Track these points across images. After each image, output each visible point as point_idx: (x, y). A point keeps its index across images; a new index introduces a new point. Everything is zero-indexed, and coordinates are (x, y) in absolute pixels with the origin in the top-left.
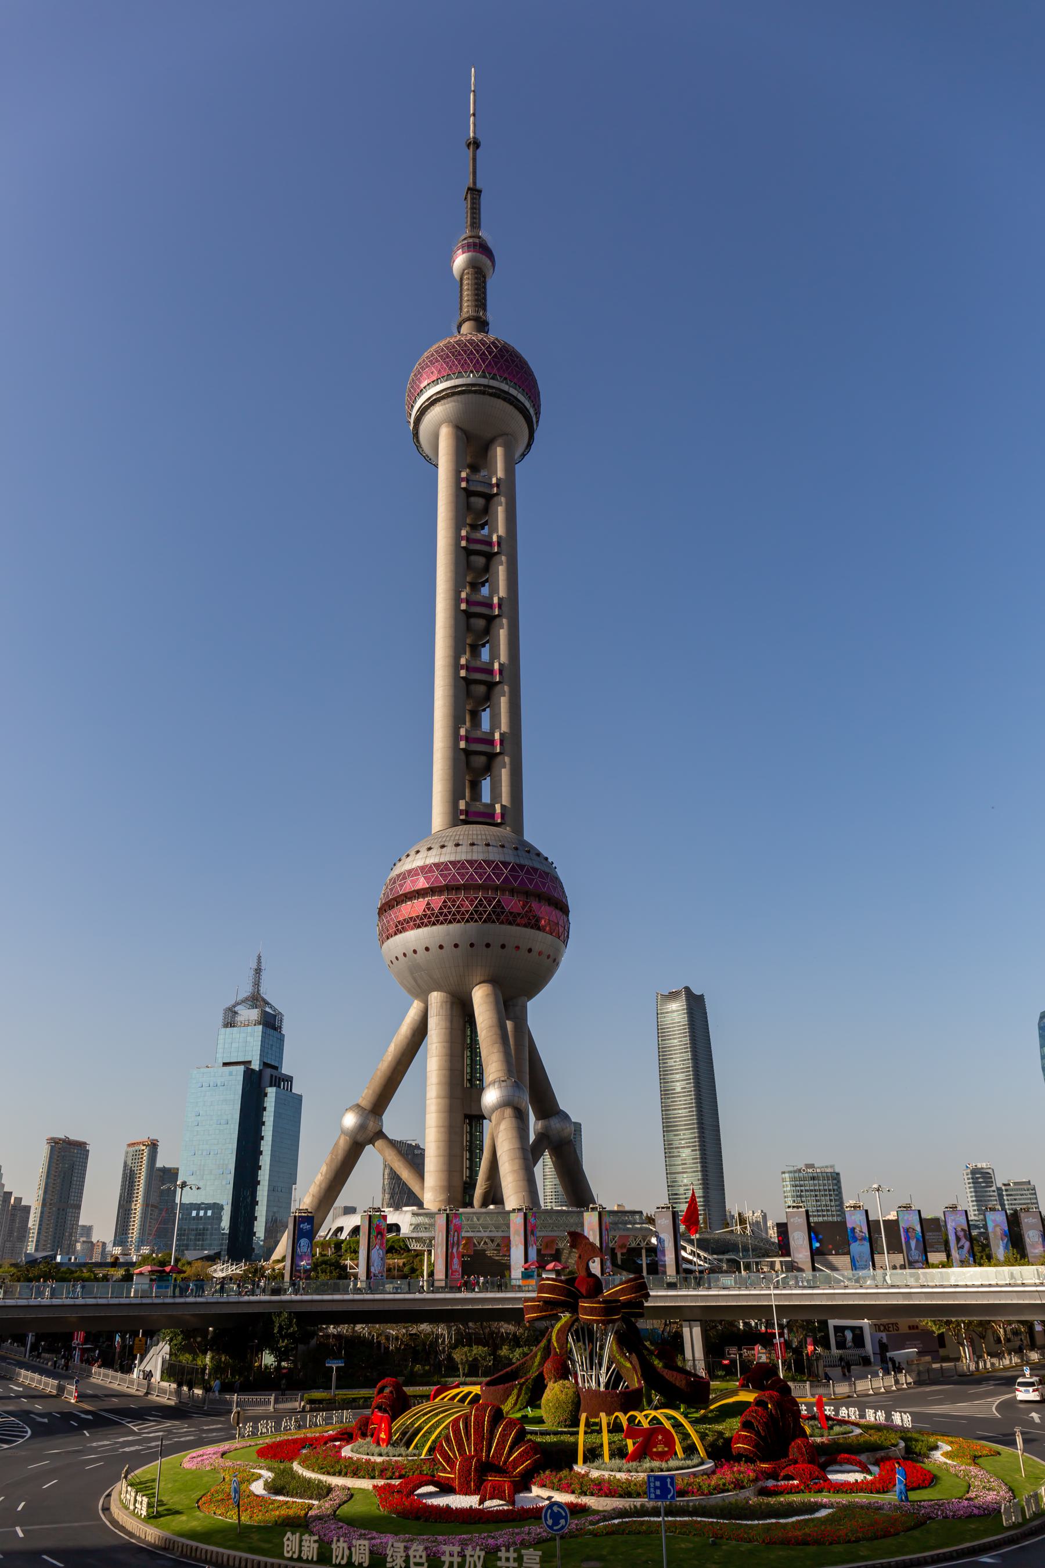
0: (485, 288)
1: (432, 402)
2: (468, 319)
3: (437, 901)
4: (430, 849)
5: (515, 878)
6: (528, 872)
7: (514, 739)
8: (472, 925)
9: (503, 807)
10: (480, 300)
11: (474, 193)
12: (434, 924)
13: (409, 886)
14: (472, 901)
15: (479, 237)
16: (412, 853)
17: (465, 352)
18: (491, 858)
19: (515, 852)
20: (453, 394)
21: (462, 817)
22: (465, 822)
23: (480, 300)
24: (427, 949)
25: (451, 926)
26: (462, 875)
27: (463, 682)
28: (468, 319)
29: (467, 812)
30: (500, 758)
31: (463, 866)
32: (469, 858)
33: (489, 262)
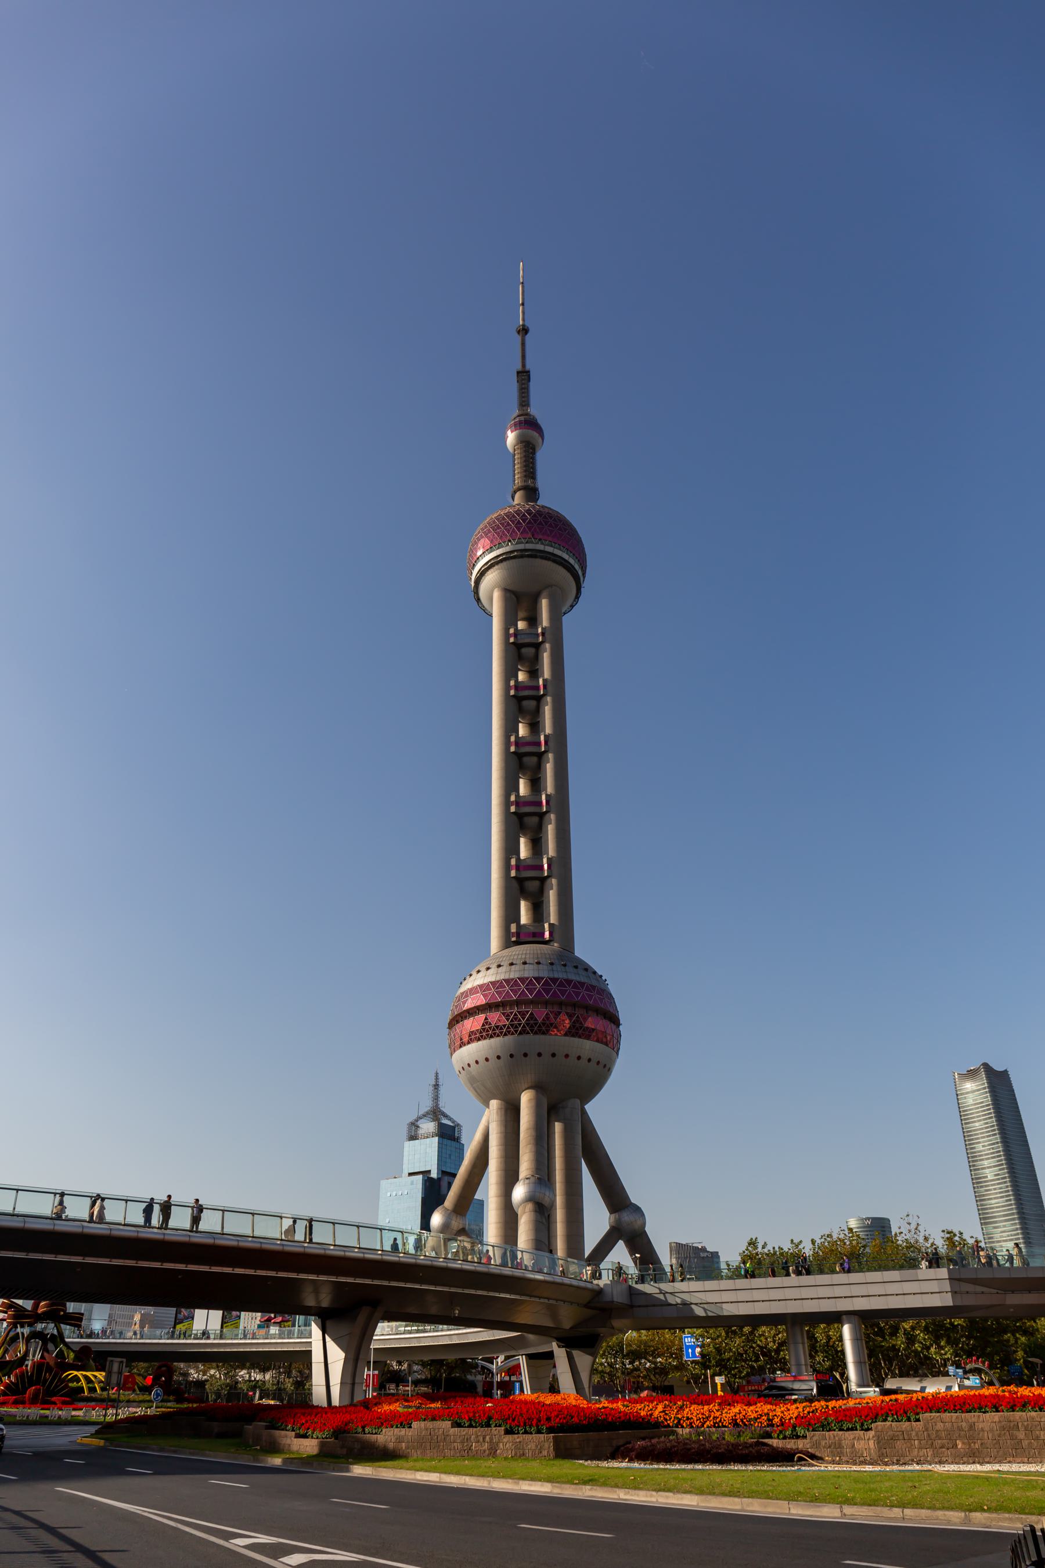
0: (533, 458)
1: (482, 573)
2: (519, 489)
3: (495, 1017)
4: (488, 969)
5: (563, 993)
6: (575, 986)
7: (563, 863)
8: (509, 1038)
9: (551, 926)
10: (530, 469)
11: (524, 376)
12: (491, 1037)
13: (469, 1004)
14: (507, 1016)
15: (527, 414)
16: (474, 973)
17: (513, 522)
18: (541, 975)
19: (550, 967)
20: (497, 563)
21: (514, 939)
22: (518, 943)
23: (530, 469)
24: (487, 1060)
25: (506, 1038)
26: (515, 992)
27: (515, 818)
28: (519, 489)
29: (518, 934)
30: (549, 881)
31: (516, 983)
32: (536, 975)
33: (535, 434)
